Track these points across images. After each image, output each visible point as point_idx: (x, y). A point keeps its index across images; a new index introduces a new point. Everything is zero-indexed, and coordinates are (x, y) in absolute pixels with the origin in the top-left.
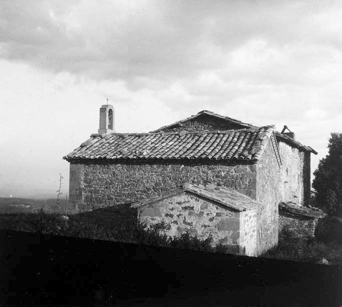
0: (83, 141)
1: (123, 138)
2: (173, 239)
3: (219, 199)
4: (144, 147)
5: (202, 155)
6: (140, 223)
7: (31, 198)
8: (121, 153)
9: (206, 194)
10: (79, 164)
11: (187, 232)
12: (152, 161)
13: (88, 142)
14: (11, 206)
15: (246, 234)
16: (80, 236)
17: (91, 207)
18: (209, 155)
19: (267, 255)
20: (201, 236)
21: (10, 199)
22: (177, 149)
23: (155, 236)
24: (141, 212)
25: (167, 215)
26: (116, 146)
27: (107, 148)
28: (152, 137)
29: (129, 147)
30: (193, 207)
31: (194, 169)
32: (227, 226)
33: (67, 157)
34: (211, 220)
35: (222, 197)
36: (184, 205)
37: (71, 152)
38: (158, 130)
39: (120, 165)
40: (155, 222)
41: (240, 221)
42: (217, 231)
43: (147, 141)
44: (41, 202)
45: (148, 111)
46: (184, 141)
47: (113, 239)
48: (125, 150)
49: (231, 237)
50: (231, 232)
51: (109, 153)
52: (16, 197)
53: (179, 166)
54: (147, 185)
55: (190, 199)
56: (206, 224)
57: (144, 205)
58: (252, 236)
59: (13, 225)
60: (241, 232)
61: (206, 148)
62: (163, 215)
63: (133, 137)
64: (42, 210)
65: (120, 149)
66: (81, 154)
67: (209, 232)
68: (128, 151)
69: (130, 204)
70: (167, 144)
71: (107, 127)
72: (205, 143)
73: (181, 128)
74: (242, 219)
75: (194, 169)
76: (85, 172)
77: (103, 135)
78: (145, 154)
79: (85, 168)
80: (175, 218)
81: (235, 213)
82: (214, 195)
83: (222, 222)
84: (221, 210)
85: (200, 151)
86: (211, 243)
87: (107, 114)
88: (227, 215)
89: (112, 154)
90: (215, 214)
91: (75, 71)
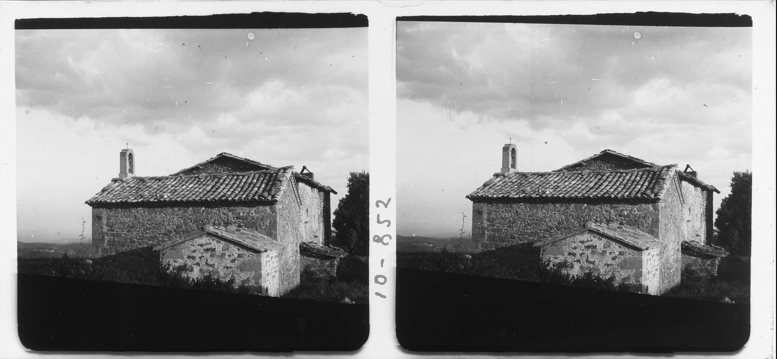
0: (487, 180)
1: (526, 177)
2: (576, 278)
3: (622, 238)
4: (547, 186)
5: (605, 194)
6: (543, 262)
7: (434, 236)
8: (524, 192)
9: (608, 233)
10: (482, 203)
11: (590, 270)
12: (554, 200)
13: (491, 181)
14: (413, 245)
15: (648, 272)
16: (482, 275)
17: (494, 246)
18: (611, 194)
19: (669, 293)
20: (604, 275)
21: (413, 238)
22: (580, 188)
23: (558, 274)
24: (544, 251)
25: (570, 254)
26: (519, 185)
27: (510, 187)
28: (555, 176)
29: (532, 186)
30: (596, 246)
31: (597, 208)
32: (629, 265)
33: (470, 196)
34: (614, 259)
35: (625, 236)
36: (586, 244)
37: (474, 191)
38: (561, 169)
39: (522, 204)
40: (558, 261)
41: (643, 259)
42: (620, 270)
43: (550, 180)
44: (444, 241)
45: (551, 150)
46: (587, 180)
47: (516, 278)
48: (528, 189)
49: (634, 276)
50: (634, 271)
51: (512, 192)
52: (419, 236)
53: (581, 205)
54: (550, 224)
55: (593, 238)
56: (609, 263)
57: (547, 244)
58: (654, 275)
59: (416, 264)
60: (643, 270)
61: (609, 187)
62: (566, 254)
63: (536, 176)
64: (445, 249)
65: (523, 188)
66: (484, 193)
67: (612, 270)
68: (531, 190)
69: (533, 243)
70: (570, 183)
71: (510, 166)
72: (608, 182)
73: (584, 168)
74: (644, 258)
75: (597, 208)
76: (488, 210)
77: (506, 174)
78: (547, 193)
79: (488, 207)
80: (578, 257)
81: (638, 252)
82: (617, 233)
83: (625, 261)
84: (623, 249)
85: (602, 190)
86: (614, 282)
87: (510, 153)
88: (630, 254)
89: (515, 193)
90: (617, 253)
91: (477, 110)
